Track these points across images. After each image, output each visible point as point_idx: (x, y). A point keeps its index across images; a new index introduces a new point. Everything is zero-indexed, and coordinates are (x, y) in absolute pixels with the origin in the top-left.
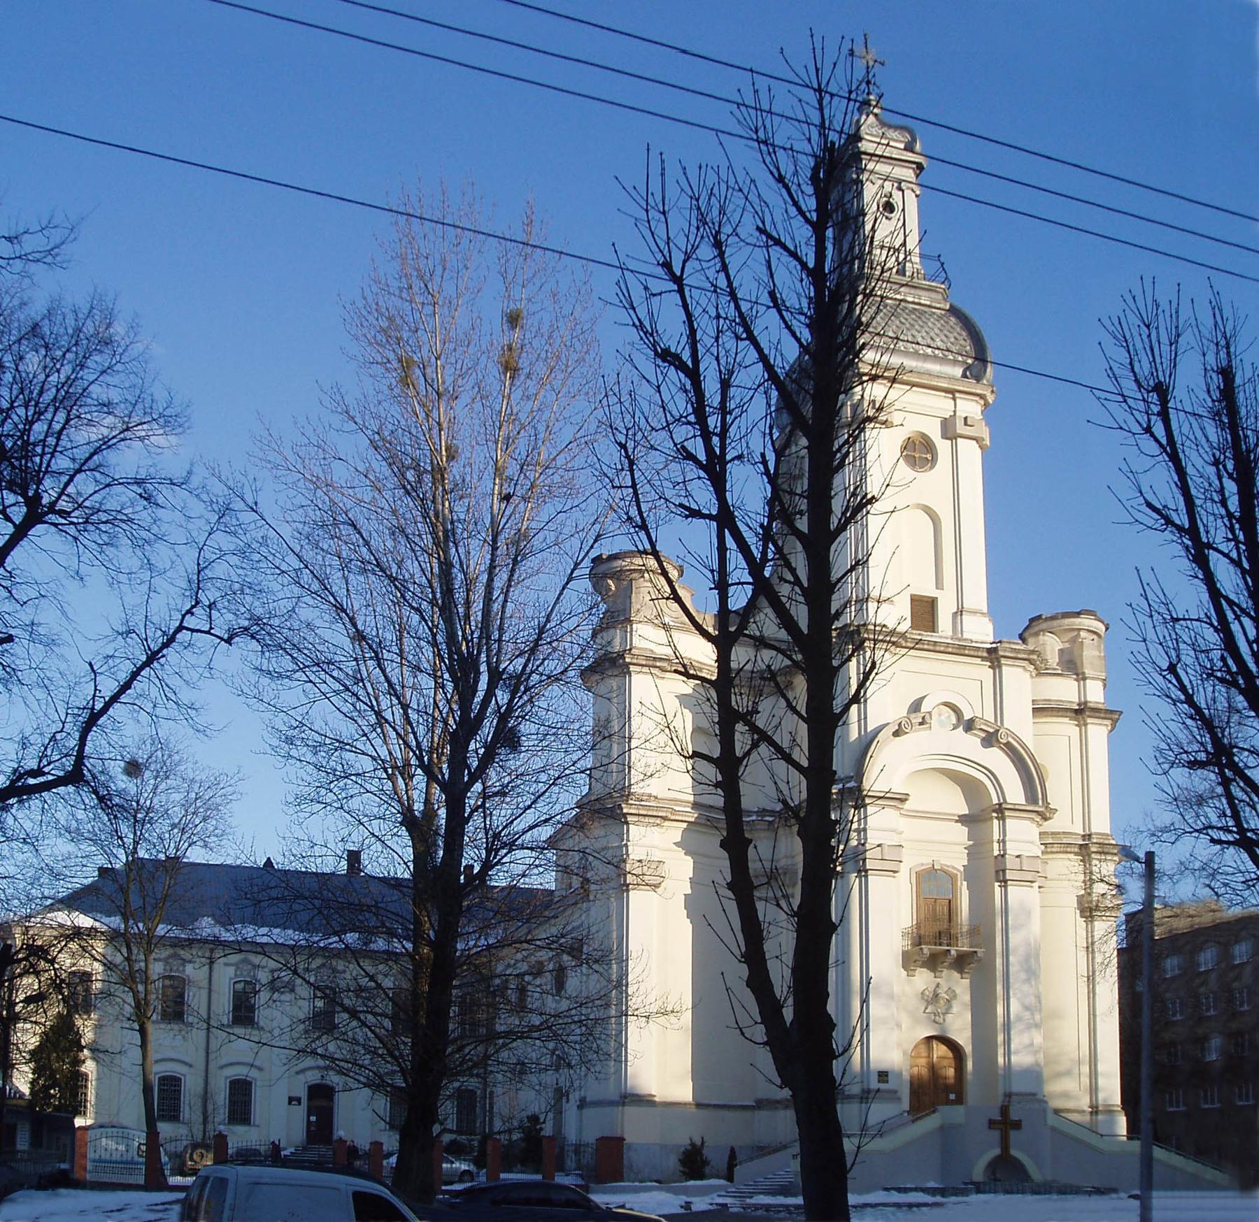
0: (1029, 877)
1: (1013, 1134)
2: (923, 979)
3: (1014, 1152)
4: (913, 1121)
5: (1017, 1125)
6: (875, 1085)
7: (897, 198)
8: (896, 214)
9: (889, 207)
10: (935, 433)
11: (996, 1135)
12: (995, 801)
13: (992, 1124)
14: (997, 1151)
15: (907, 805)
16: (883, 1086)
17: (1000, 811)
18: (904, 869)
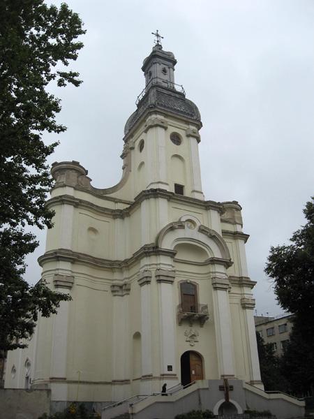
0: (225, 287)
1: (230, 393)
2: (186, 328)
3: (230, 401)
4: (184, 388)
5: (232, 388)
6: (166, 372)
7: (167, 69)
8: (168, 73)
9: (164, 71)
10: (182, 133)
11: (222, 394)
12: (210, 257)
13: (221, 388)
14: (224, 400)
15: (176, 257)
16: (170, 372)
17: (214, 261)
18: (177, 280)
